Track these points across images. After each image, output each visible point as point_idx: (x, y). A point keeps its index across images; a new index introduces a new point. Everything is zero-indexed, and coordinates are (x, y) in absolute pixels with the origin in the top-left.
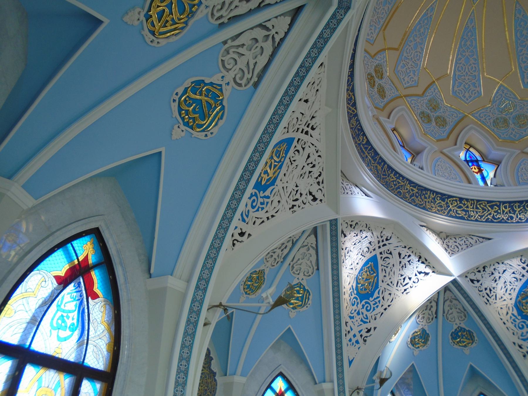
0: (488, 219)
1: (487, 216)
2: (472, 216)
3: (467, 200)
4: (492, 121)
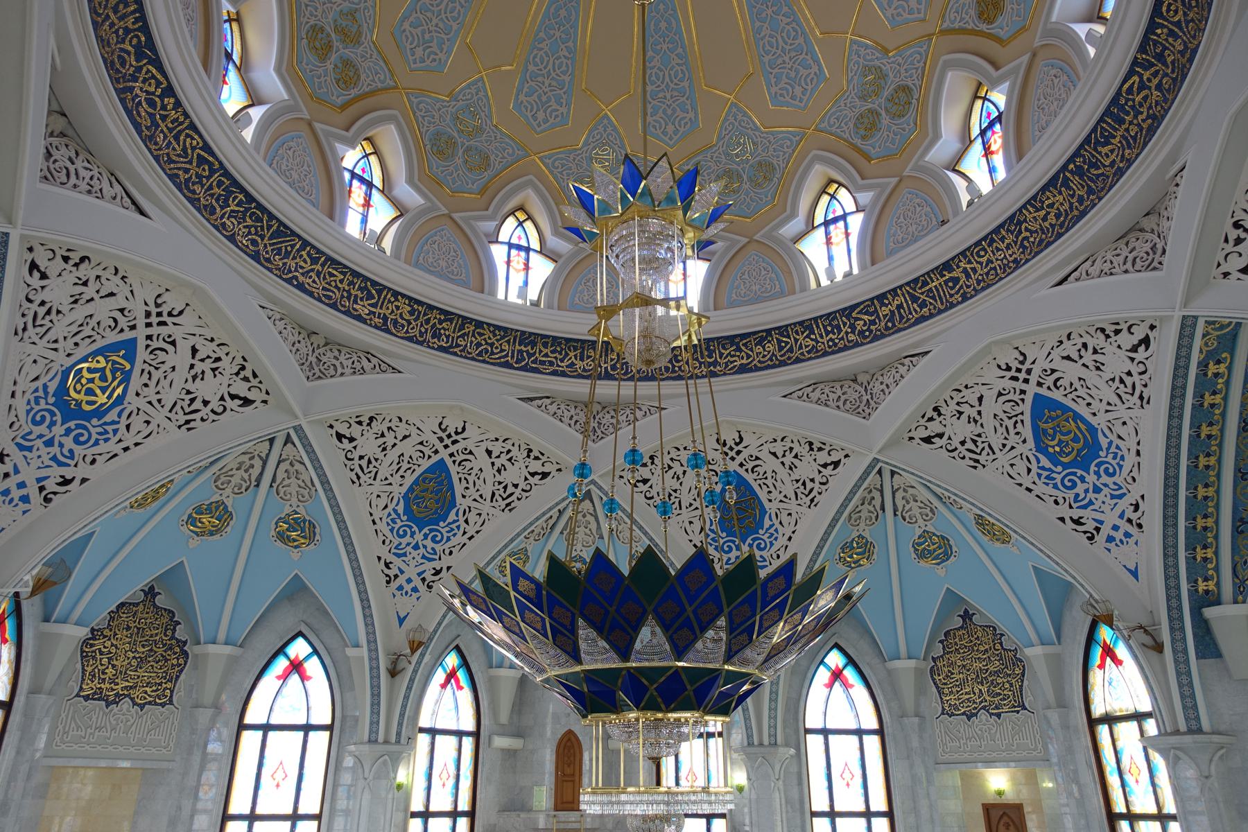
0: (177, 176)
1: (179, 169)
2: (156, 144)
3: (178, 104)
4: (312, 22)
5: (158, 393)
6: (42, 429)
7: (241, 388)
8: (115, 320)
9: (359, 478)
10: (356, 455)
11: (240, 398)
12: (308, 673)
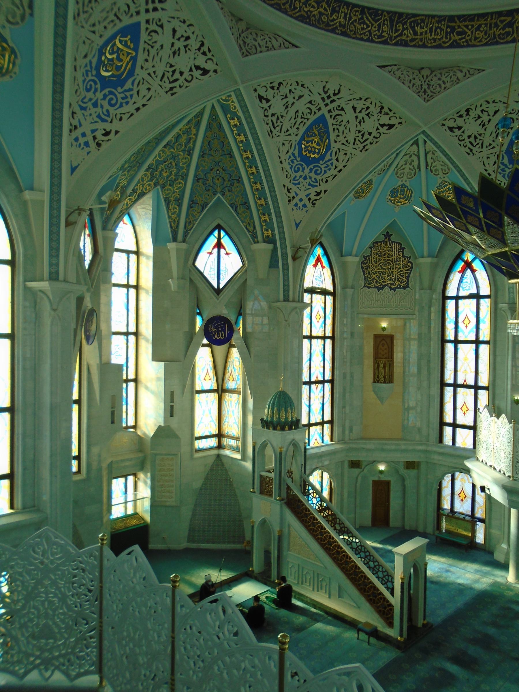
5: (345, 137)
6: (300, 173)
7: (385, 120)
8: (310, 109)
9: (471, 150)
10: (465, 136)
11: (387, 126)
12: (475, 268)
